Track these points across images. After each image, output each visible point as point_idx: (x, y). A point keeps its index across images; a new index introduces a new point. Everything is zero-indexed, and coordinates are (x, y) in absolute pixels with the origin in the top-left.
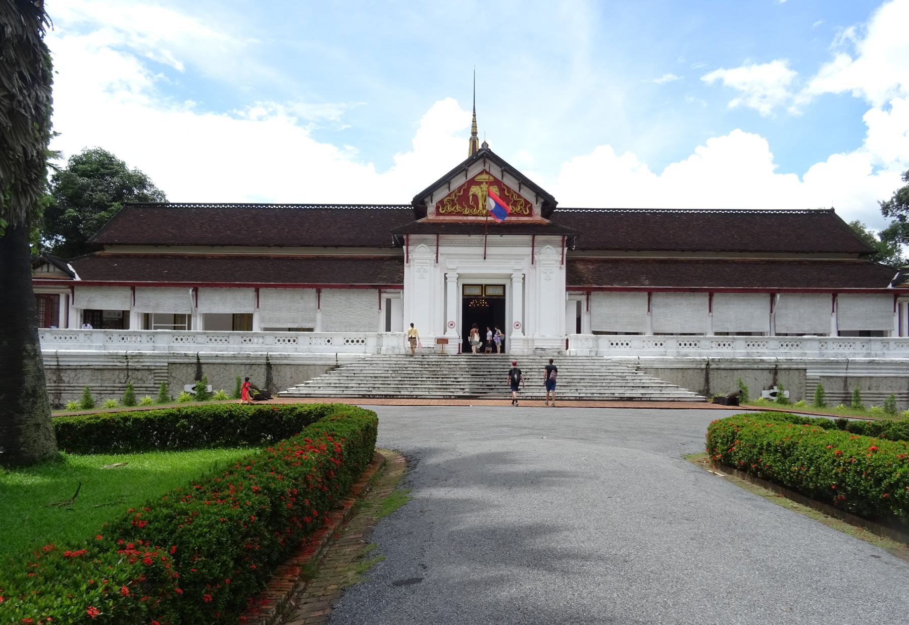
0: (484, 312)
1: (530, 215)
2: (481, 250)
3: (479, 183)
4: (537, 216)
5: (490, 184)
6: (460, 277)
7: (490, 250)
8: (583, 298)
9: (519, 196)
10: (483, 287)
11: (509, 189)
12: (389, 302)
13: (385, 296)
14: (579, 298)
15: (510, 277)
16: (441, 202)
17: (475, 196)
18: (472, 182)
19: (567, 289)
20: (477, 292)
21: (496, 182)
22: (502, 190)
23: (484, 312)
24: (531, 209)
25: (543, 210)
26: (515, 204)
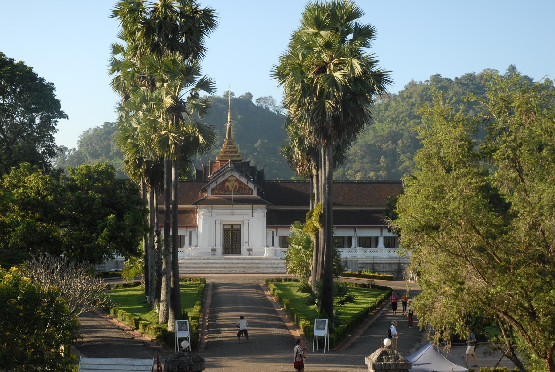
0: (232, 240)
1: (252, 194)
2: (230, 211)
3: (230, 181)
4: (255, 195)
5: (235, 181)
6: (221, 221)
7: (234, 211)
8: (275, 230)
9: (247, 186)
10: (232, 225)
11: (243, 183)
12: (191, 232)
13: (189, 230)
14: (273, 230)
15: (243, 222)
16: (213, 190)
17: (228, 186)
18: (227, 180)
19: (267, 227)
20: (229, 227)
21: (237, 180)
22: (239, 184)
23: (232, 240)
24: (252, 192)
25: (257, 192)
26: (245, 190)
